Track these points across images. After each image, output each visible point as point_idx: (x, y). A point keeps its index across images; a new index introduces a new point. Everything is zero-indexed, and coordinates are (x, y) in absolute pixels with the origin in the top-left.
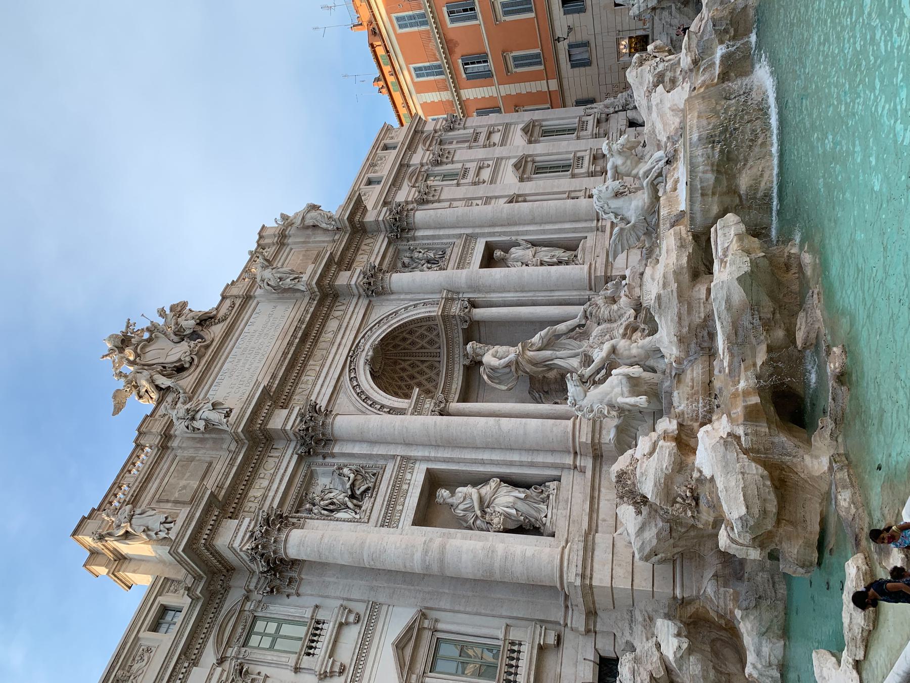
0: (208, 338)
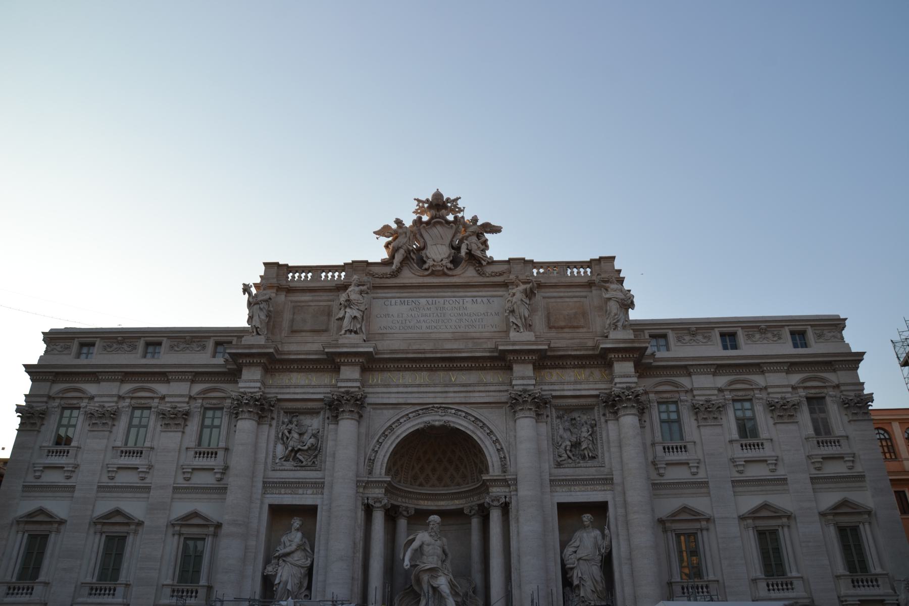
0: (458, 271)
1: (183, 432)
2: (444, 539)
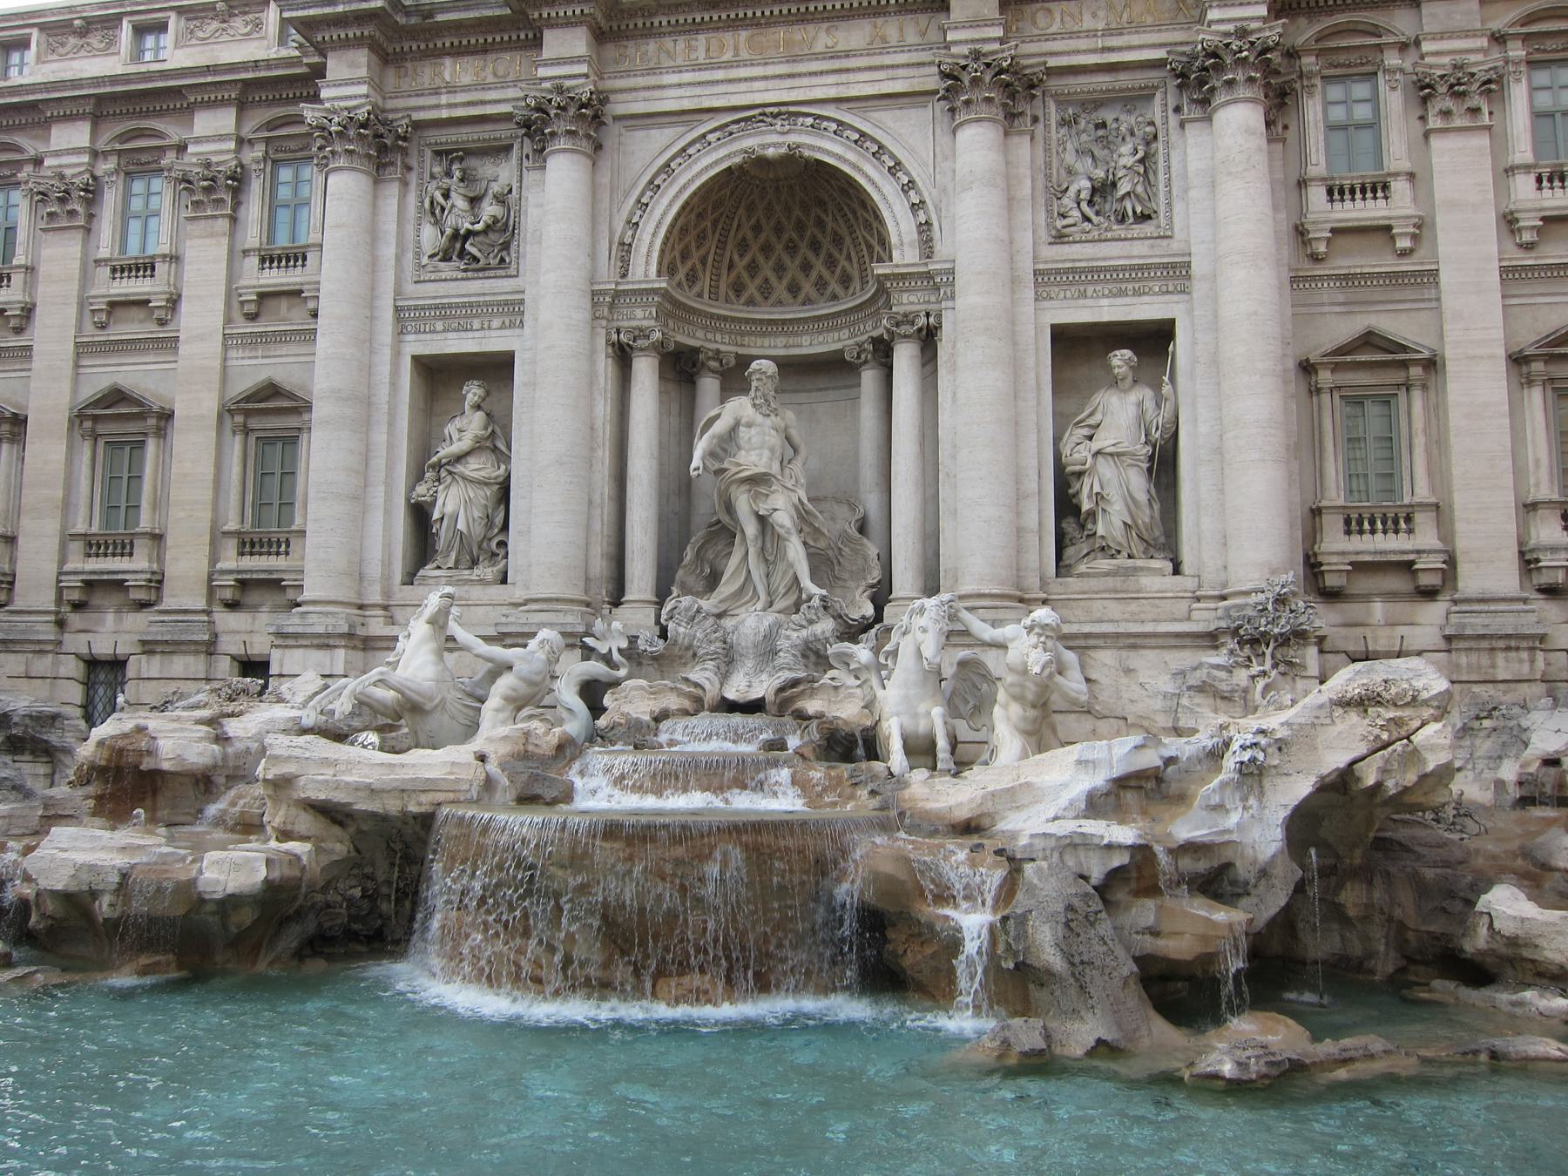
1: (234, 220)
2: (790, 415)
